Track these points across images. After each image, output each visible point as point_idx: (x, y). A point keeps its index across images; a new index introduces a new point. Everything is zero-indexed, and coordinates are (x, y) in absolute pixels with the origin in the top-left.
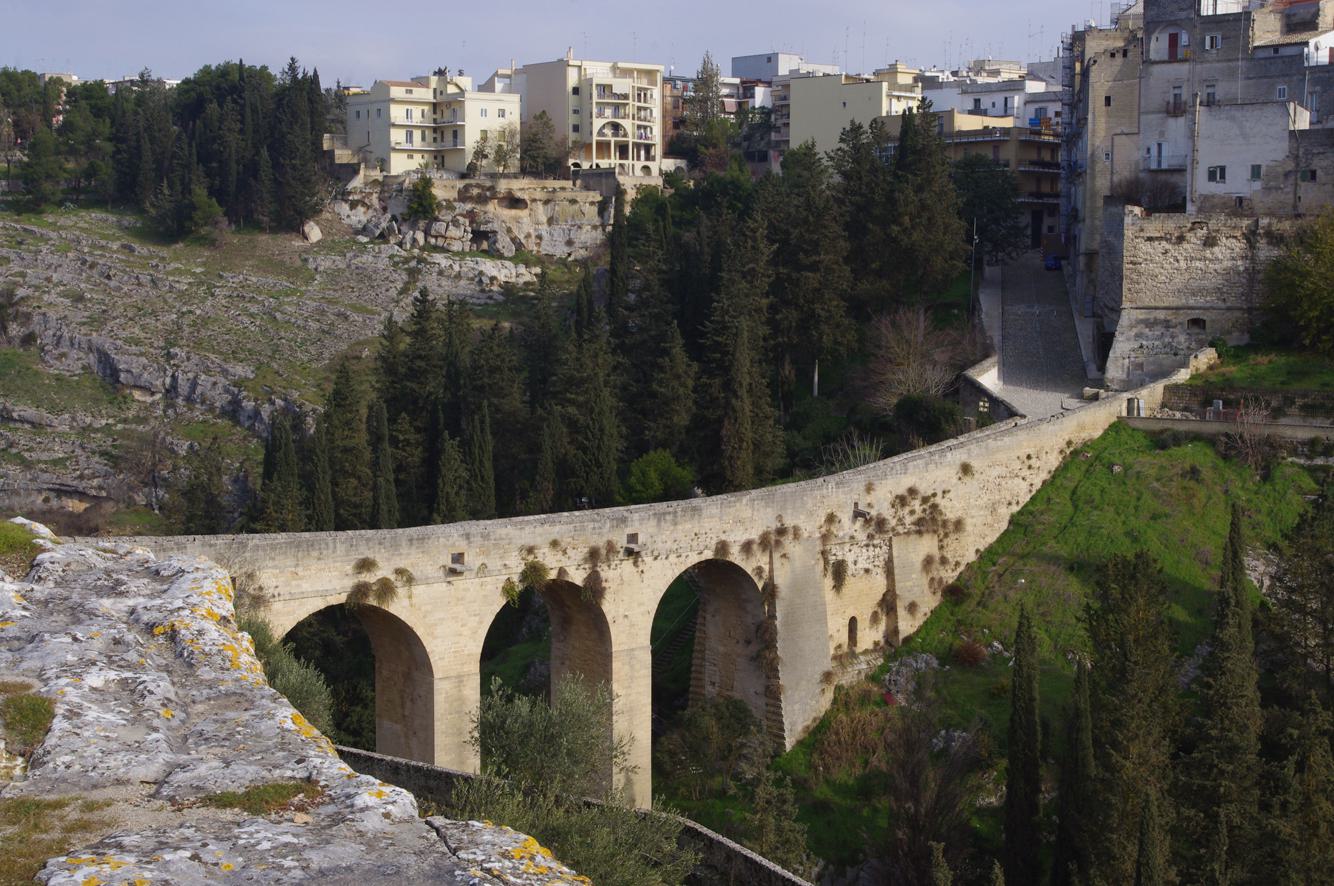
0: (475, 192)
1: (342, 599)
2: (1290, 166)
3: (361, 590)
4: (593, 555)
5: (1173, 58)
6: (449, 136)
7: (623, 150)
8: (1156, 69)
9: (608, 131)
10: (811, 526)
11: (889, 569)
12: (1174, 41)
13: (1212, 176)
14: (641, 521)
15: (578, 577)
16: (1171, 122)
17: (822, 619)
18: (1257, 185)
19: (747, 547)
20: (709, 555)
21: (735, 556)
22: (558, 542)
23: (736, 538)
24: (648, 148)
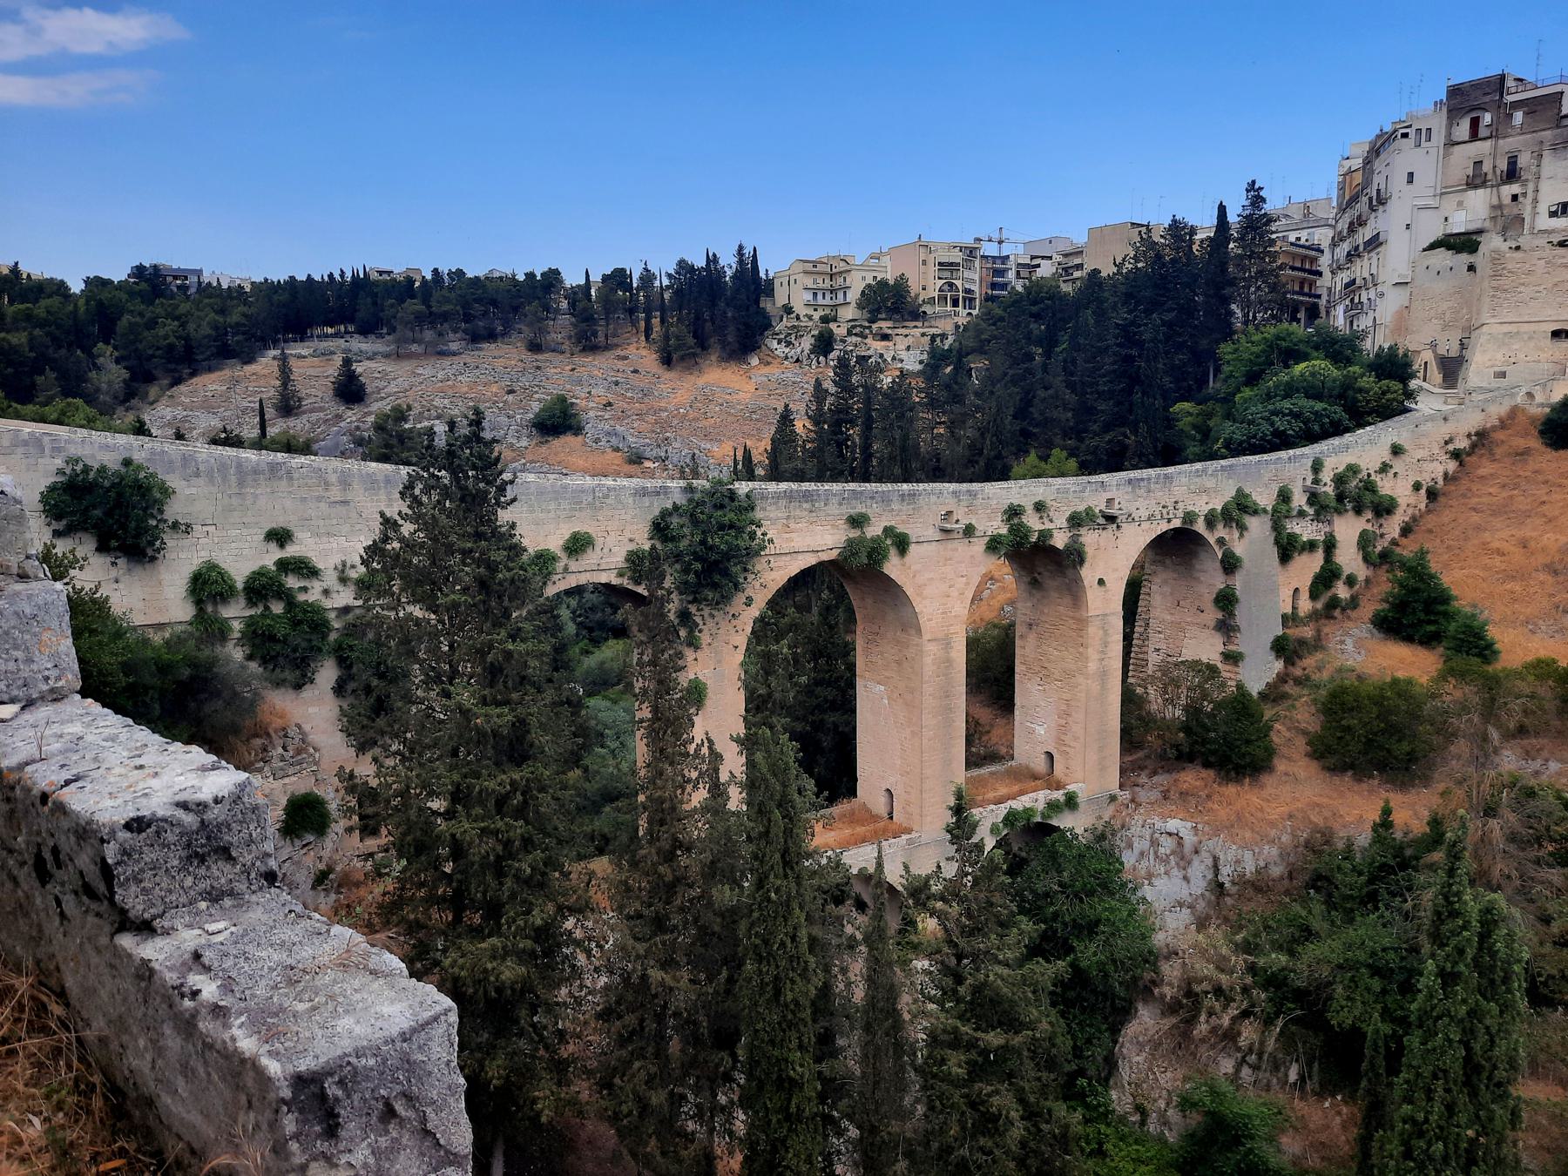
0: (858, 330)
1: (833, 555)
3: (851, 547)
4: (1076, 521)
5: (1474, 136)
6: (840, 295)
7: (955, 303)
9: (946, 287)
10: (1265, 498)
11: (1330, 545)
12: (1475, 123)
14: (1110, 489)
15: (1060, 541)
16: (1471, 193)
17: (1274, 590)
19: (1210, 522)
20: (1177, 523)
21: (1200, 527)
22: (1051, 497)
23: (1201, 506)
24: (972, 300)
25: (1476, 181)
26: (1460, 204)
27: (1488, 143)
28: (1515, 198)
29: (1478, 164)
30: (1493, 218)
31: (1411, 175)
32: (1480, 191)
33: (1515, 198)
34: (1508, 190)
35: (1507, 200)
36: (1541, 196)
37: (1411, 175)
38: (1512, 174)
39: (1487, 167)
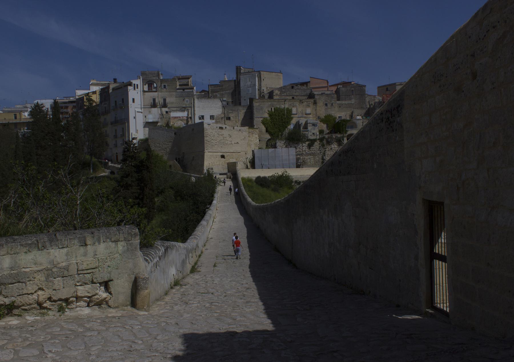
2: (223, 116)
8: (146, 93)
13: (200, 119)
16: (153, 109)
18: (214, 121)
25: (154, 105)
26: (150, 112)
27: (156, 93)
28: (167, 112)
29: (154, 100)
30: (161, 118)
31: (133, 99)
32: (156, 109)
33: (167, 112)
34: (164, 110)
35: (164, 113)
36: (196, 112)
37: (133, 99)
38: (165, 105)
39: (157, 101)
